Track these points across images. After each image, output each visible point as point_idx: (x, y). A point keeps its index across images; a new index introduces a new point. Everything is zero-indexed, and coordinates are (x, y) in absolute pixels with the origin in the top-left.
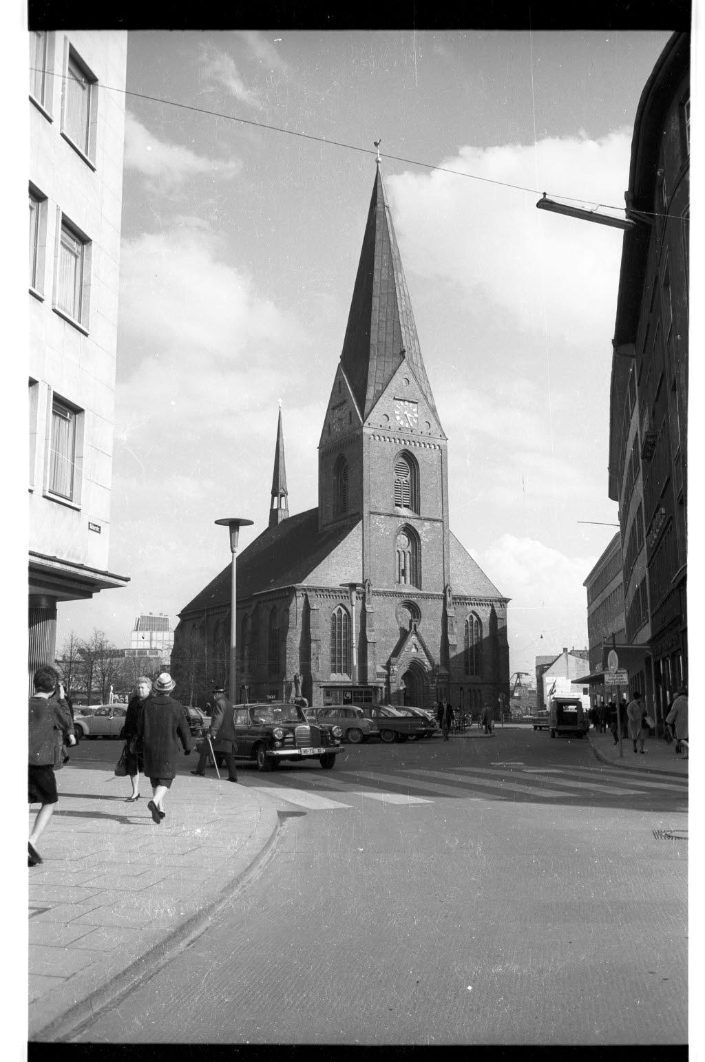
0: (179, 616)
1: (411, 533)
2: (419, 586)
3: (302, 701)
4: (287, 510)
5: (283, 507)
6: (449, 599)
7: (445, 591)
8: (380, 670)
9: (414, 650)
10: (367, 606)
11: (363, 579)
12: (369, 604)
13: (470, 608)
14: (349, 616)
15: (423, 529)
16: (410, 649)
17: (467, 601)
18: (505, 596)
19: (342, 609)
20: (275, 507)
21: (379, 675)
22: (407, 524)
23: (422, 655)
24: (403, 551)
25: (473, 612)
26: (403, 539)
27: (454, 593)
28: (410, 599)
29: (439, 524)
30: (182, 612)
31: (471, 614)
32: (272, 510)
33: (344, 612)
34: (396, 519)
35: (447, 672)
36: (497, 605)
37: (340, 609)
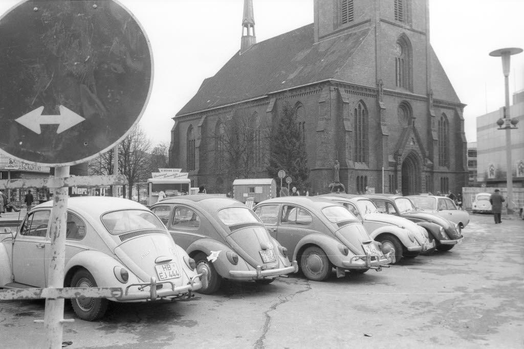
0: (174, 119)
1: (404, 42)
2: (412, 91)
3: (340, 187)
4: (254, 37)
5: (251, 34)
6: (431, 102)
7: (428, 95)
8: (391, 159)
9: (412, 144)
10: (381, 103)
11: (376, 79)
12: (382, 101)
13: (443, 110)
14: (366, 112)
15: (414, 39)
16: (410, 142)
17: (441, 105)
18: (462, 102)
19: (361, 104)
20: (245, 34)
21: (390, 164)
22: (404, 33)
23: (416, 147)
24: (399, 59)
25: (444, 114)
26: (397, 50)
27: (434, 97)
28: (407, 100)
29: (423, 37)
30: (176, 115)
31: (442, 116)
32: (243, 37)
33: (363, 108)
34: (397, 27)
35: (432, 163)
36: (458, 109)
37: (359, 105)
